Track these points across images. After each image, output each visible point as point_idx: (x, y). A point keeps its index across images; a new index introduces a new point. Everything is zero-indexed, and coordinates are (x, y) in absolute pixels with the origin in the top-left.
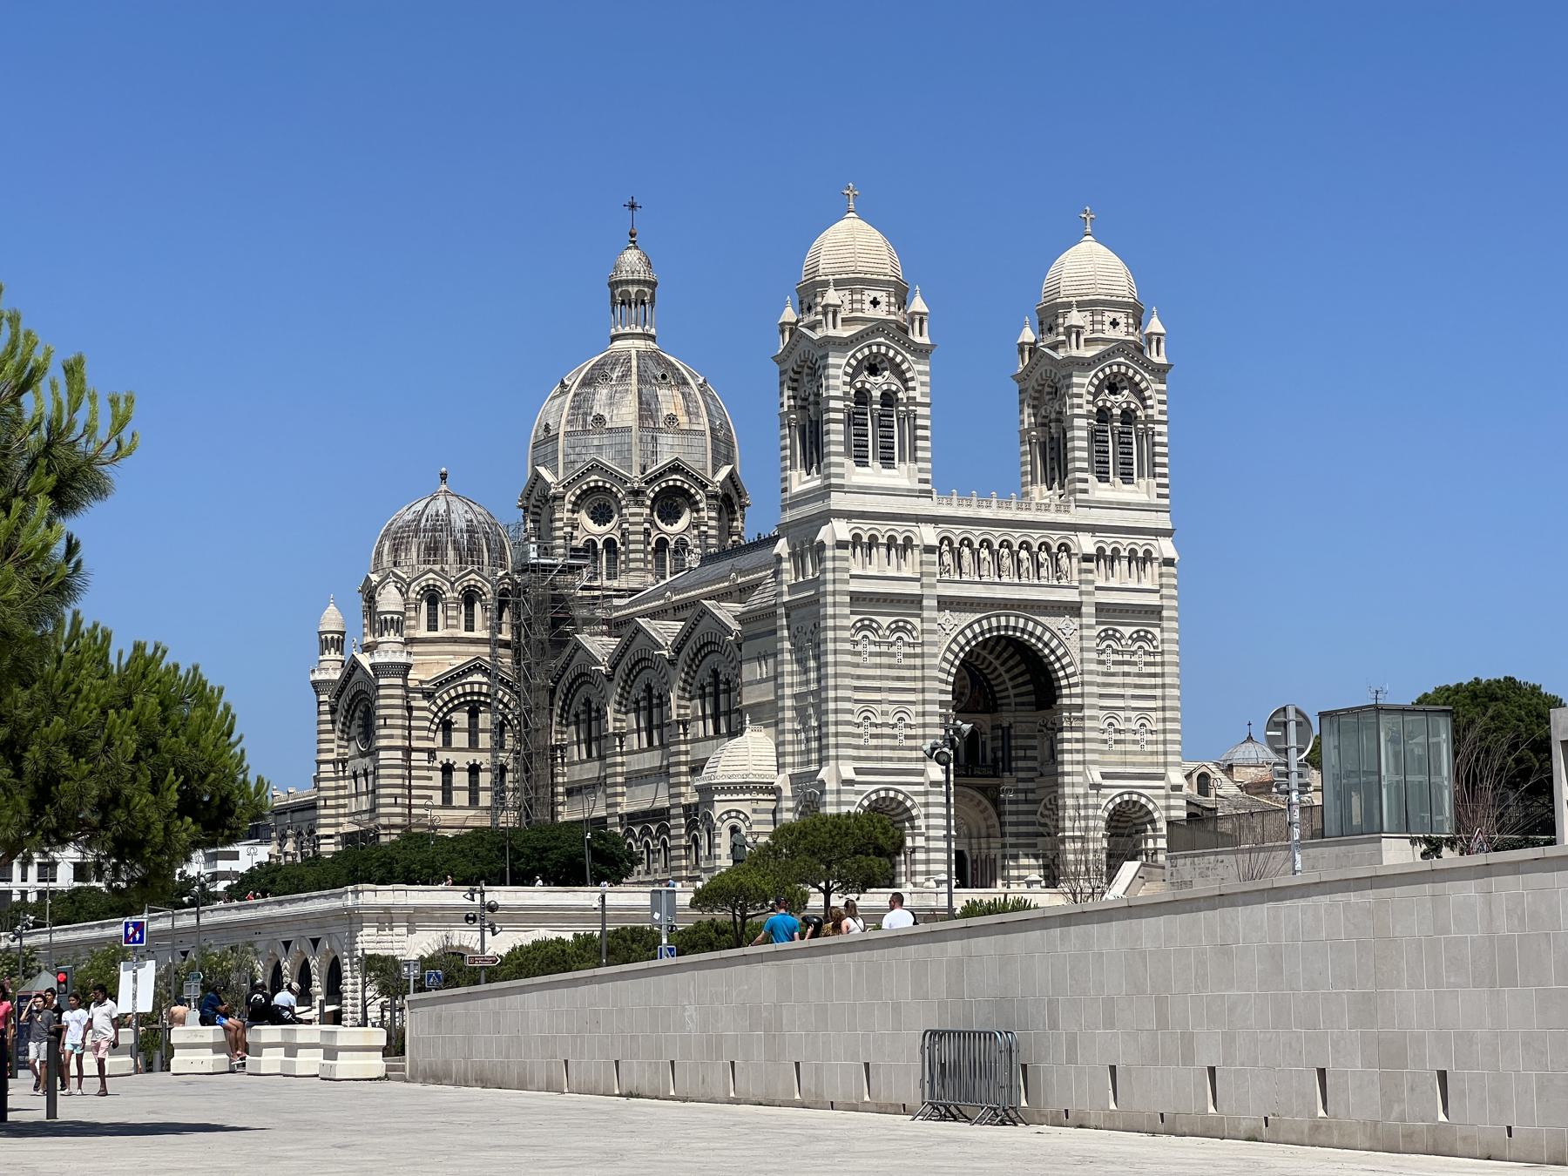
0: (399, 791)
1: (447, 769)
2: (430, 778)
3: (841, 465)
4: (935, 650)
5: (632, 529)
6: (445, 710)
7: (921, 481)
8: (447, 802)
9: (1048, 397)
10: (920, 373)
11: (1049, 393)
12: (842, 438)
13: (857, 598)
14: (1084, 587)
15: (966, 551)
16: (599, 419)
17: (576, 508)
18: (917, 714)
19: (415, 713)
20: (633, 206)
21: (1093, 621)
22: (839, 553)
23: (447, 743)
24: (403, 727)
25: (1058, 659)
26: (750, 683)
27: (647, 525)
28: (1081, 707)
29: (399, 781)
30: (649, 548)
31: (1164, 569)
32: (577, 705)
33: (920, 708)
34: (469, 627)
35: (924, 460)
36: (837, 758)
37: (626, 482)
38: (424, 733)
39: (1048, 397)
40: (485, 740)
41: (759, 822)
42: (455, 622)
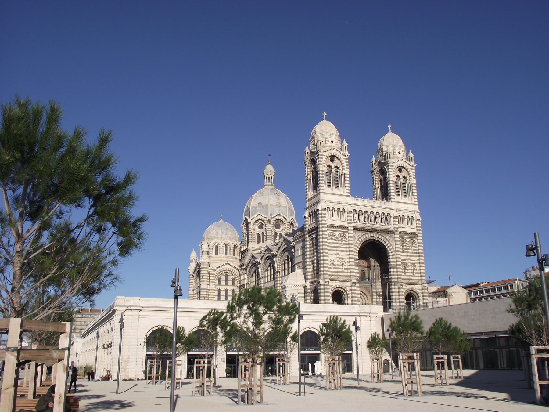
0: (205, 296)
1: (219, 291)
2: (214, 293)
3: (323, 187)
4: (352, 242)
5: (268, 230)
6: (219, 274)
7: (347, 193)
8: (219, 299)
13: (328, 226)
14: (395, 226)
15: (361, 214)
16: (260, 203)
18: (348, 262)
19: (210, 275)
20: (269, 155)
21: (398, 236)
22: (323, 212)
23: (219, 283)
24: (207, 279)
25: (389, 247)
26: (297, 257)
27: (272, 229)
29: (206, 293)
30: (273, 235)
31: (418, 222)
33: (348, 260)
34: (226, 253)
36: (324, 274)
38: (213, 281)
40: (230, 283)
41: (300, 297)
42: (222, 252)
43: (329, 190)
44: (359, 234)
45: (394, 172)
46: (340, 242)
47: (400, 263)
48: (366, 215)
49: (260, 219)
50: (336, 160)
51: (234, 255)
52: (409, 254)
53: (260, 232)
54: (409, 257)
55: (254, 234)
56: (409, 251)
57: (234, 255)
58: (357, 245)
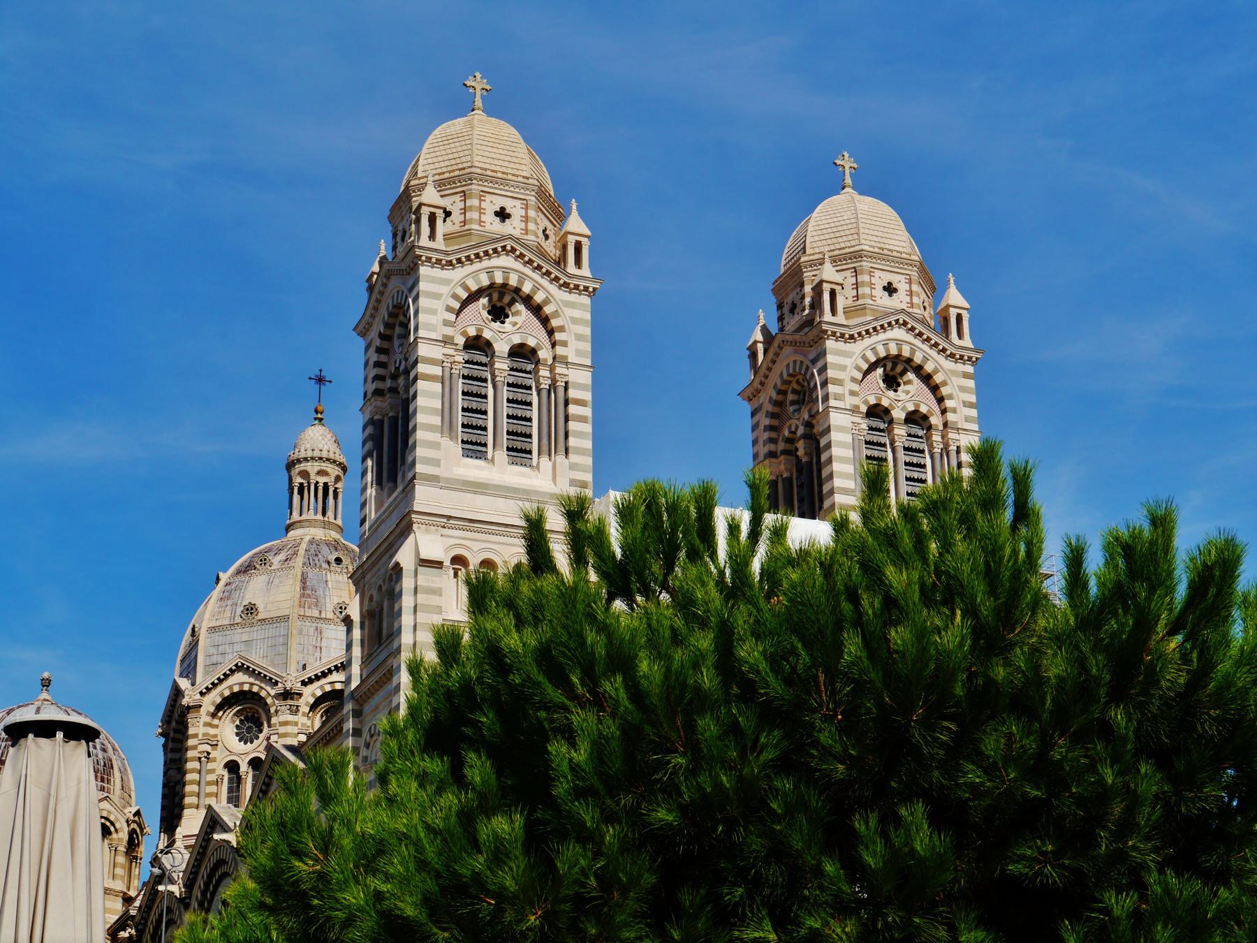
3: (436, 446)
9: (792, 409)
10: (575, 321)
11: (793, 403)
12: (437, 404)
16: (251, 609)
17: (216, 722)
20: (320, 380)
35: (580, 451)
37: (276, 683)
39: (792, 409)
43: (473, 469)
45: (856, 387)
49: (246, 687)
50: (521, 315)
53: (244, 752)
55: (210, 766)
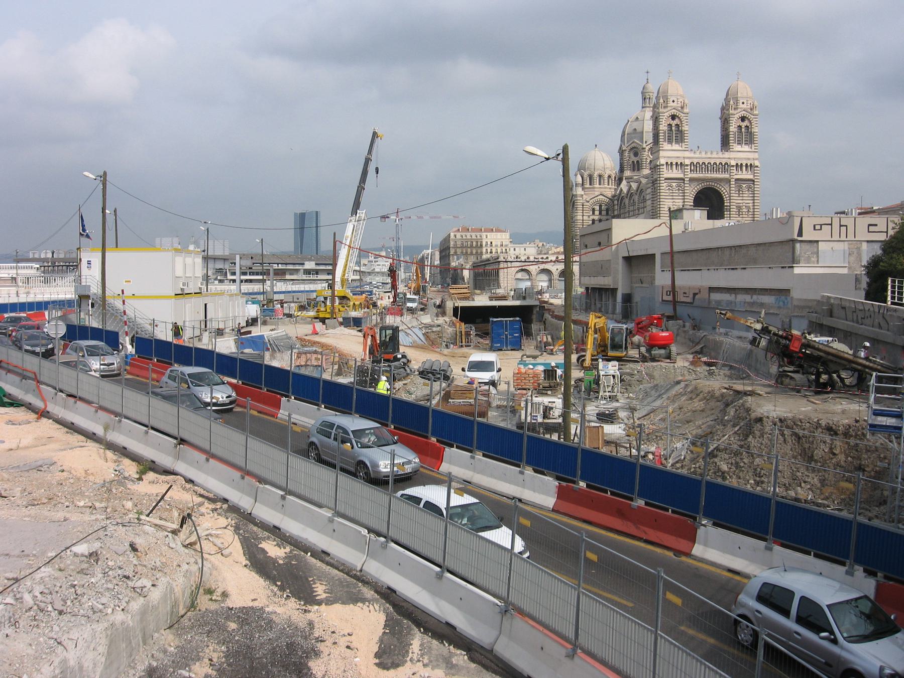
16: (635, 129)
20: (647, 72)
23: (593, 213)
28: (730, 206)
32: (623, 205)
40: (604, 213)
44: (696, 183)
46: (677, 191)
47: (734, 207)
48: (704, 166)
51: (608, 185)
52: (744, 198)
54: (744, 201)
56: (744, 195)
57: (608, 185)
58: (693, 193)
